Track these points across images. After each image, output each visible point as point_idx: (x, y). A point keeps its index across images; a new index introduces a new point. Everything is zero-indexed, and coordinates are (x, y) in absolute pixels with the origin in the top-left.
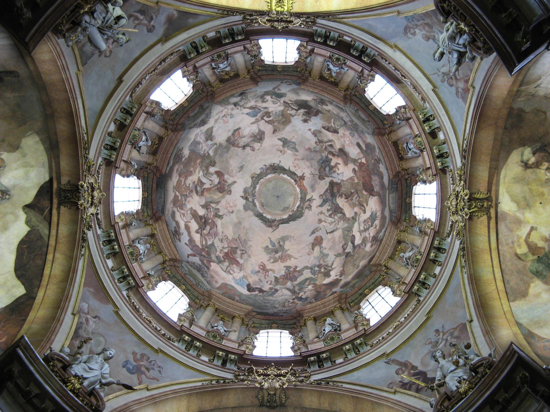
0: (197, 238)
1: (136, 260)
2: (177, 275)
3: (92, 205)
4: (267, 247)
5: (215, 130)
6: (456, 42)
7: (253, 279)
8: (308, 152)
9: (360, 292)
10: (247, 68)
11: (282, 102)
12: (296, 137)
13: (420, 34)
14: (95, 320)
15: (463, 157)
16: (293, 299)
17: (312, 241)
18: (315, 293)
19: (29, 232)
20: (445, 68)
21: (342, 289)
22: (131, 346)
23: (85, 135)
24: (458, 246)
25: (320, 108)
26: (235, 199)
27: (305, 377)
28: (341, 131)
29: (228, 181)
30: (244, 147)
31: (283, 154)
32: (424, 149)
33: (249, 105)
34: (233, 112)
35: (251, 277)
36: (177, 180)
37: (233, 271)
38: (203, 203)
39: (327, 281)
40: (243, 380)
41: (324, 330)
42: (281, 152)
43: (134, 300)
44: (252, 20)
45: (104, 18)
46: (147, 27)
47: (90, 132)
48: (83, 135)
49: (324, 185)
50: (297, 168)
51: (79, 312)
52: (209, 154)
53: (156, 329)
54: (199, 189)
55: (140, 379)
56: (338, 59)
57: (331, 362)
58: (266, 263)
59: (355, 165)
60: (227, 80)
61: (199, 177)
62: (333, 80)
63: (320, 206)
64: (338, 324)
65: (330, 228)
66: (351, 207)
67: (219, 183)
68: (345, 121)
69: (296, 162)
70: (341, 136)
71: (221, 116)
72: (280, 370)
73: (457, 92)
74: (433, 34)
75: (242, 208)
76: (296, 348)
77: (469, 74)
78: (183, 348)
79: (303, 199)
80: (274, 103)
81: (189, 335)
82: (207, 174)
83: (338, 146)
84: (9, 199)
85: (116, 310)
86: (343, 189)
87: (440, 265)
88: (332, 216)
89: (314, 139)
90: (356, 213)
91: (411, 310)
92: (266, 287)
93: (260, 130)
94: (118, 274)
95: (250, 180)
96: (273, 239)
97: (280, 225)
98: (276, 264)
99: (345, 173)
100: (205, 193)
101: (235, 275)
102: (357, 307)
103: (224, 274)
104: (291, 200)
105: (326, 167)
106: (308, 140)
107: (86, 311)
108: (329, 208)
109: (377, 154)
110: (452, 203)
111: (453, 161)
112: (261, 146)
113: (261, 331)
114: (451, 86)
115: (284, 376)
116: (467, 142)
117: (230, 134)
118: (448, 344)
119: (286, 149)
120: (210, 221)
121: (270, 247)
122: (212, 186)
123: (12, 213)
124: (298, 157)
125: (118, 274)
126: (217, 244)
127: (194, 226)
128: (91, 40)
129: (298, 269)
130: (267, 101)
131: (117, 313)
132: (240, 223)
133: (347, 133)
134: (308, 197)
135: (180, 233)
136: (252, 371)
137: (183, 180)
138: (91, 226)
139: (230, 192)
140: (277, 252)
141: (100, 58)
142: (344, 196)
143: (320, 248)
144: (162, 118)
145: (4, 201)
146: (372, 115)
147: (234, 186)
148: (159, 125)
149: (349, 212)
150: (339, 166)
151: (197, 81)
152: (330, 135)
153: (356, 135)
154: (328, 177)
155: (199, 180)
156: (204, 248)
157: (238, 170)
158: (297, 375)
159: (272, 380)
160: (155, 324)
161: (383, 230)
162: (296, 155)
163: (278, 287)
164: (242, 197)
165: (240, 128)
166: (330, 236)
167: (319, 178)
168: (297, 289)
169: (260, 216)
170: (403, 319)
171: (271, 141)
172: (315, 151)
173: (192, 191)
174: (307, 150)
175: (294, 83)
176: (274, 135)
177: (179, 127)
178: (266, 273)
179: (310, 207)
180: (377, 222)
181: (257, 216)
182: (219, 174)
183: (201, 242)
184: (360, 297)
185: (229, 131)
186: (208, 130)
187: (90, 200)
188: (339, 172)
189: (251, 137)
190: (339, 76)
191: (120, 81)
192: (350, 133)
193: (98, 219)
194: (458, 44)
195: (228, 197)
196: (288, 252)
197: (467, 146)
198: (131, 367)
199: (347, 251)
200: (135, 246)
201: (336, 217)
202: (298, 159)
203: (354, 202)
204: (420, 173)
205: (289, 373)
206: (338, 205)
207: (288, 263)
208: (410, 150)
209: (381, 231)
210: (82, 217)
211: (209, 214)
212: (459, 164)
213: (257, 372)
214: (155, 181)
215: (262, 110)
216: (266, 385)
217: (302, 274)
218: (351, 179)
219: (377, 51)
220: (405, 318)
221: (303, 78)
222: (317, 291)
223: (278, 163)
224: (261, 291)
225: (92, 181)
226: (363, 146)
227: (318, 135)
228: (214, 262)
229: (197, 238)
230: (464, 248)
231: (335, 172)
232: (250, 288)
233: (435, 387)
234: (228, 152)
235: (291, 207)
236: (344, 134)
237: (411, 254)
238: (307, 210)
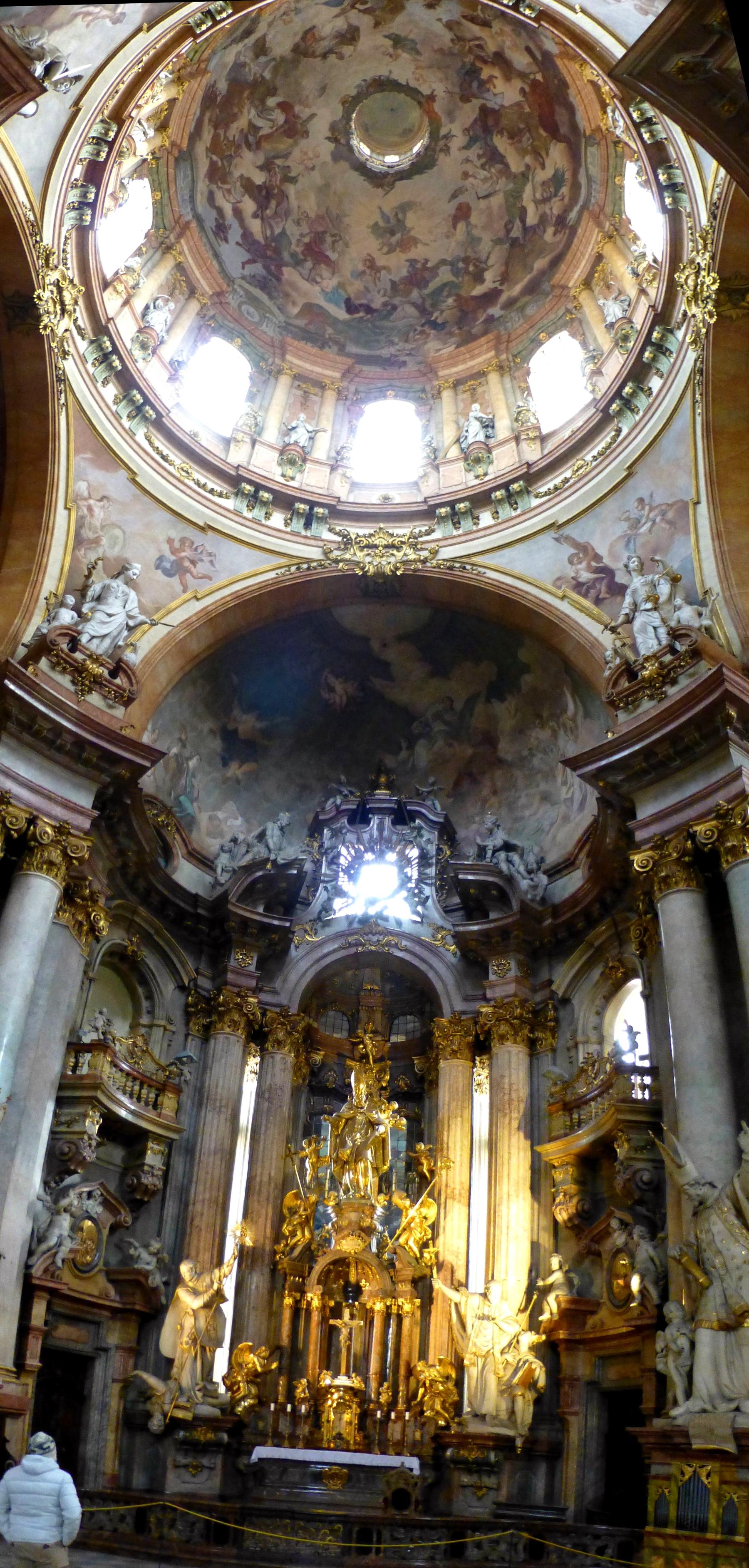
22: (165, 530)
40: (337, 561)
58: (376, 255)
92: (377, 304)
95: (340, 109)
98: (393, 255)
101: (325, 283)
103: (305, 285)
163: (397, 301)
168: (428, 304)
216: (371, 570)
224: (369, 309)
232: (351, 307)
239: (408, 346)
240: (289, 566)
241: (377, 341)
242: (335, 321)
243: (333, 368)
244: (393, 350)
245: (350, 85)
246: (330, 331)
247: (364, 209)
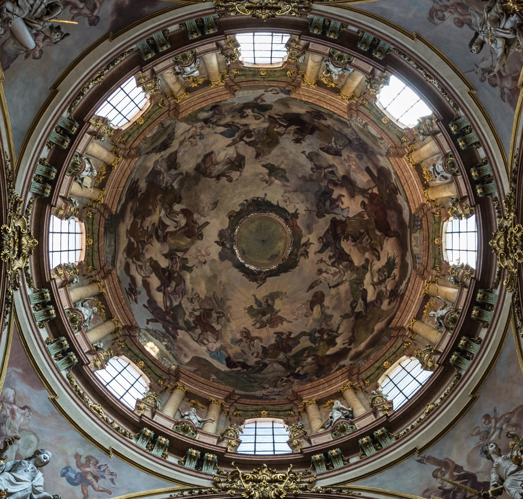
0: (159, 297)
1: (80, 329)
3: (19, 256)
4: (252, 307)
5: (180, 154)
6: (501, 27)
7: (234, 350)
8: (301, 182)
9: (377, 365)
10: (220, 73)
11: (267, 117)
12: (285, 162)
13: (450, 18)
15: (513, 180)
16: (288, 377)
17: (310, 299)
18: (316, 367)
20: (484, 62)
21: (352, 362)
23: (8, 163)
24: (510, 300)
25: (315, 123)
26: (209, 245)
27: (309, 482)
28: (345, 153)
29: (198, 221)
30: (218, 177)
31: (270, 185)
32: (457, 172)
33: (223, 122)
34: (203, 132)
35: (231, 348)
36: (131, 222)
37: (208, 340)
38: (166, 251)
39: (331, 351)
41: (331, 417)
42: (267, 182)
43: (76, 381)
44: (227, 8)
45: (32, 6)
46: (89, 17)
47: (15, 160)
48: (5, 163)
49: (322, 225)
50: (288, 203)
52: (173, 187)
53: (107, 421)
54: (160, 232)
56: (340, 57)
57: (344, 461)
58: (251, 328)
59: (364, 197)
60: (195, 89)
61: (160, 218)
62: (333, 85)
63: (321, 251)
64: (350, 409)
65: (334, 280)
66: (360, 252)
67: (186, 225)
68: (350, 140)
69: (287, 194)
70: (345, 159)
71: (188, 137)
72: (274, 473)
73: (503, 94)
74: (468, 17)
75: (216, 257)
76: (295, 442)
77: (518, 69)
78: (144, 446)
79: (296, 243)
80: (256, 118)
81: (151, 428)
82: (170, 213)
83: (341, 172)
85: (53, 397)
86: (349, 229)
87: (487, 327)
88: (336, 264)
89: (309, 165)
90: (367, 260)
91: (449, 388)
92: (252, 361)
93: (238, 155)
96: (259, 297)
97: (268, 279)
98: (264, 330)
99: (351, 207)
100: (169, 239)
101: (210, 345)
102: (373, 385)
103: (194, 345)
104: (281, 244)
105: (325, 201)
106: (302, 166)
108: (332, 254)
109: (393, 181)
110: (498, 243)
111: (498, 186)
112: (240, 175)
113: (247, 421)
114: (495, 85)
115: (281, 482)
116: (518, 160)
117: (200, 160)
118: (504, 434)
119: (273, 178)
120: (176, 275)
121: (255, 307)
122: (178, 228)
124: (288, 188)
126: (187, 305)
127: (155, 282)
128: (14, 35)
129: (292, 336)
130: (248, 115)
131: (54, 401)
132: (215, 277)
133: (353, 155)
134: (304, 240)
135: (136, 292)
136: (237, 476)
137: (139, 221)
139: (201, 236)
140: (264, 314)
141: (27, 60)
142: (350, 238)
143: (321, 308)
144: (110, 140)
146: (386, 130)
147: (207, 228)
148: (107, 150)
149: (357, 260)
150: (343, 199)
151: (156, 91)
152: (330, 159)
153: (365, 158)
154: (329, 213)
155: (160, 221)
156: (168, 310)
157: (211, 207)
158: (298, 480)
159: (265, 487)
160: (105, 413)
161: (405, 282)
162: (287, 186)
163: (267, 361)
164: (217, 242)
165: (212, 152)
166: (333, 291)
167: (317, 215)
168: (292, 362)
169: (241, 267)
170: (439, 401)
171: (253, 168)
172: (311, 180)
173: (151, 236)
174: (300, 178)
175: (282, 91)
176: (258, 160)
177: (133, 152)
178: (250, 342)
179: (306, 254)
180: (396, 271)
181: (237, 267)
182: (186, 213)
183: (165, 303)
184: (377, 372)
185: (198, 156)
186: (171, 155)
188: (343, 207)
189: (227, 163)
190: (342, 79)
192: (357, 156)
193: (27, 275)
194: (503, 29)
195: (199, 243)
196: (279, 314)
197: (517, 165)
199: (356, 310)
200: (77, 310)
201: (341, 266)
202: (289, 192)
203: (365, 245)
204: (454, 205)
205: (288, 478)
206: (343, 250)
207: (280, 328)
208: (439, 174)
209: (401, 284)
210: (6, 273)
211: (175, 266)
212: (507, 190)
213: (244, 477)
214: (103, 223)
215: (241, 127)
217: (299, 343)
218: (360, 215)
219: (393, 44)
220: (441, 399)
221: (294, 84)
222: (319, 365)
223: (263, 196)
224: (244, 365)
226: (375, 172)
227: (315, 159)
228: (181, 329)
229: (159, 297)
230: (518, 302)
231: (338, 206)
232: (230, 363)
233: (491, 495)
234: (197, 184)
235: (281, 254)
236: (348, 156)
237: (445, 311)
238: (302, 258)
239: (276, 390)
240: (183, 491)
241: (252, 387)
242: (218, 372)
243: (218, 394)
244: (264, 392)
245: (235, 201)
246: (214, 377)
247: (242, 296)
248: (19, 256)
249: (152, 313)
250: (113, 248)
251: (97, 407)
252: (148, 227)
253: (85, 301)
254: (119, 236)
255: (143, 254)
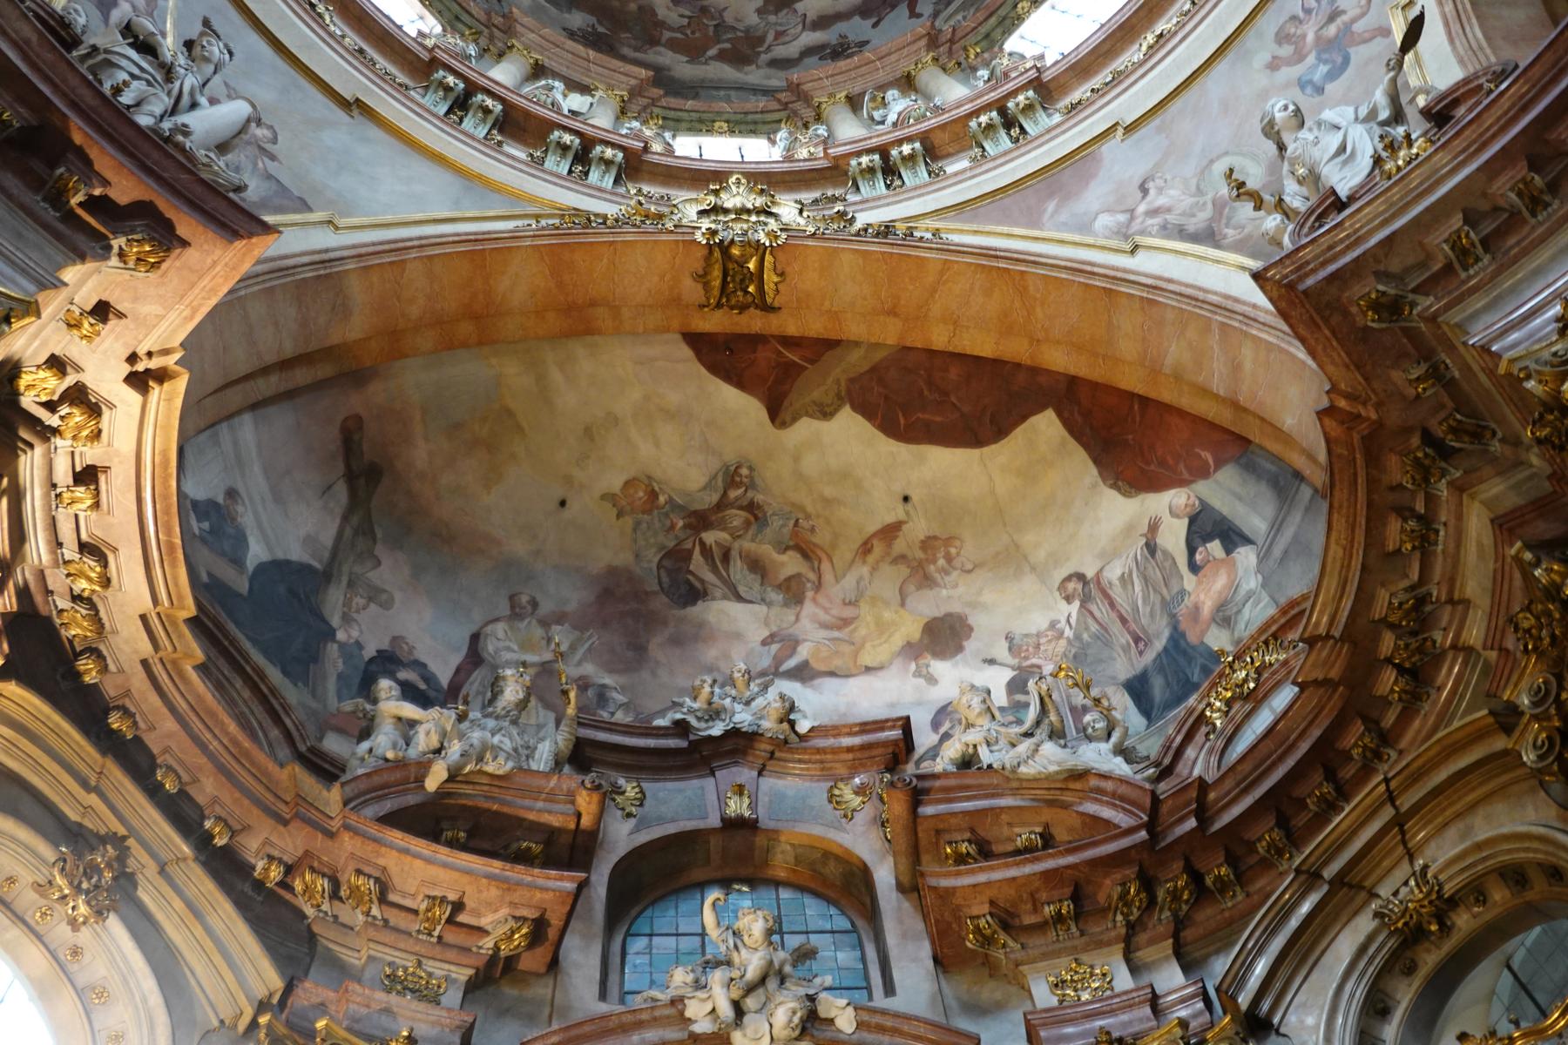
2: (983, 30)
3: (770, 214)
14: (1152, 192)
19: (854, 408)
23: (543, 222)
48: (543, 228)
51: (1126, 237)
55: (1367, 35)
84: (751, 469)
85: (1120, 131)
94: (996, 142)
107: (1122, 218)
123: (797, 459)
125: (996, 142)
131: (1130, 129)
135: (842, 45)
137: (667, 35)
138: (841, 215)
145: (758, 481)
177: (498, 20)
187: (754, 218)
191: (355, 106)
198: (1323, 69)
225: (691, 212)
248: (770, 214)
249: (893, 7)
250: (733, 93)
251: (1151, 38)
252: (682, 16)
253: (872, 119)
254: (703, 81)
255: (747, 30)
